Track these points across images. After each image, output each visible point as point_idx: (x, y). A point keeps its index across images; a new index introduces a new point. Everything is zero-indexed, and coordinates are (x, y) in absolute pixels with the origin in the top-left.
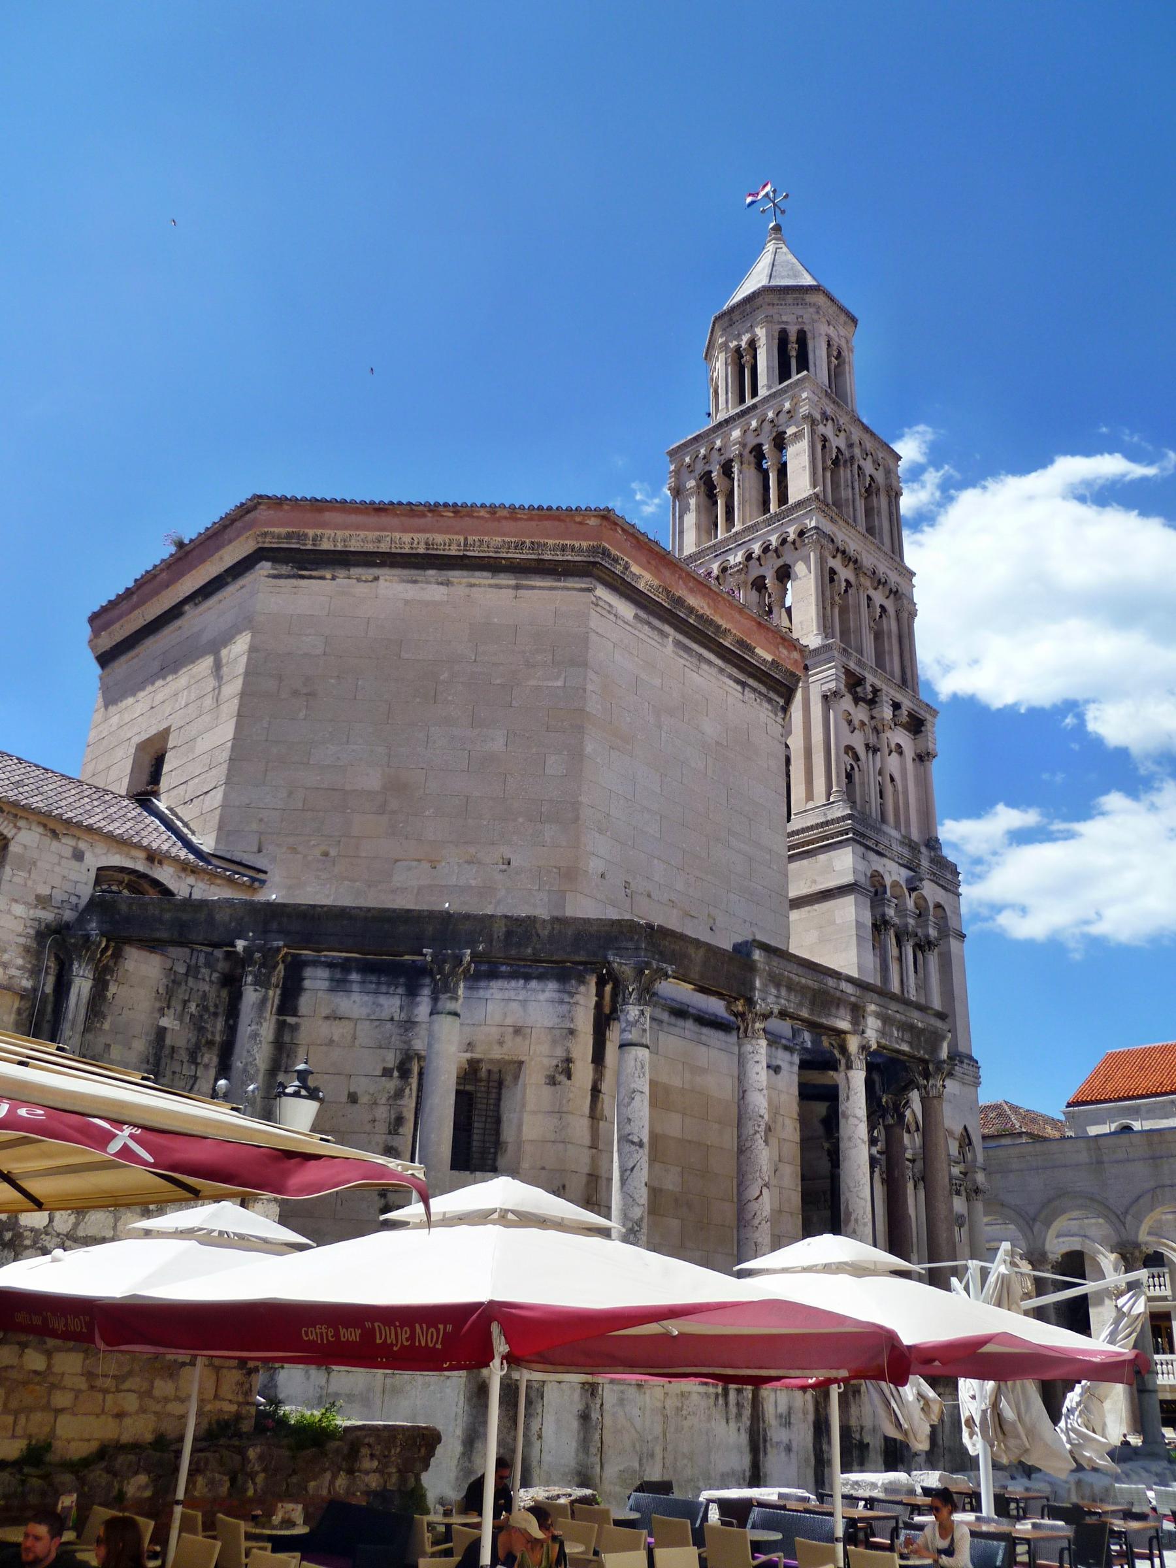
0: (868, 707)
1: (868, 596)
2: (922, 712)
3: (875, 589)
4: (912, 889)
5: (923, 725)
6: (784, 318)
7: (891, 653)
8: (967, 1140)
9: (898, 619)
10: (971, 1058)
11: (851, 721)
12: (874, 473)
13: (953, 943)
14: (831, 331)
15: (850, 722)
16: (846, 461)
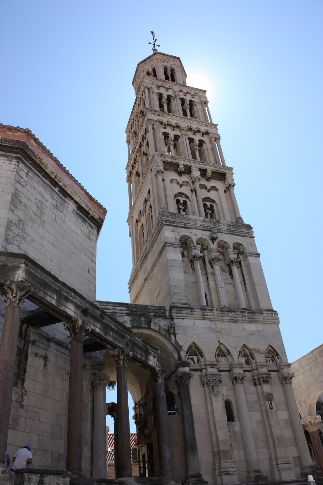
0: (189, 176)
1: (189, 138)
2: (222, 170)
3: (194, 135)
4: (213, 239)
5: (225, 175)
6: (147, 68)
7: (208, 156)
8: (275, 354)
9: (211, 142)
10: (272, 310)
11: (179, 183)
12: (193, 99)
13: (251, 260)
14: (166, 64)
15: (178, 183)
16: (174, 98)
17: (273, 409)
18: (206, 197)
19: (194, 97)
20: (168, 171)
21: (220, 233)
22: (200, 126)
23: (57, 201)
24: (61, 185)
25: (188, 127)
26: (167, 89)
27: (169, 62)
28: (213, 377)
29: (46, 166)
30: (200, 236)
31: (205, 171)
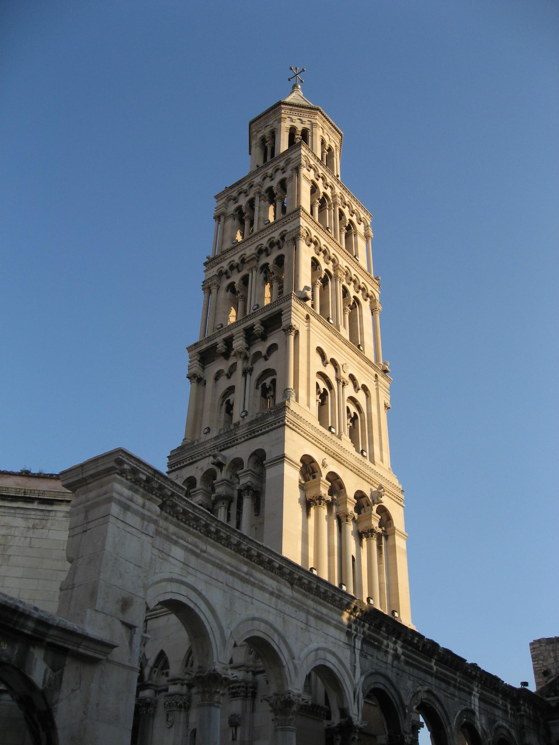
2: (276, 309)
3: (268, 255)
17: (236, 739)
18: (263, 372)
19: (283, 171)
20: (215, 360)
21: (235, 447)
22: (272, 232)
23: (34, 519)
24: (37, 497)
25: (256, 252)
26: (246, 193)
27: (267, 124)
28: (168, 700)
29: (7, 490)
30: (205, 470)
31: (252, 328)
